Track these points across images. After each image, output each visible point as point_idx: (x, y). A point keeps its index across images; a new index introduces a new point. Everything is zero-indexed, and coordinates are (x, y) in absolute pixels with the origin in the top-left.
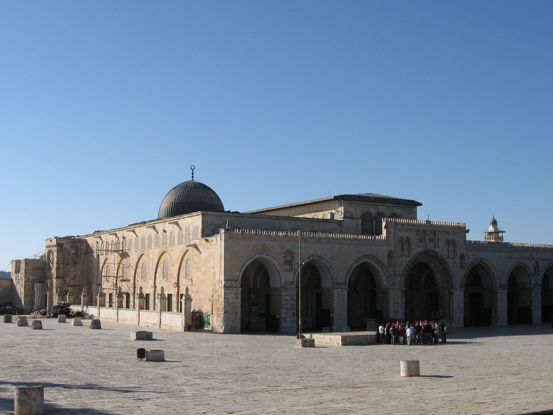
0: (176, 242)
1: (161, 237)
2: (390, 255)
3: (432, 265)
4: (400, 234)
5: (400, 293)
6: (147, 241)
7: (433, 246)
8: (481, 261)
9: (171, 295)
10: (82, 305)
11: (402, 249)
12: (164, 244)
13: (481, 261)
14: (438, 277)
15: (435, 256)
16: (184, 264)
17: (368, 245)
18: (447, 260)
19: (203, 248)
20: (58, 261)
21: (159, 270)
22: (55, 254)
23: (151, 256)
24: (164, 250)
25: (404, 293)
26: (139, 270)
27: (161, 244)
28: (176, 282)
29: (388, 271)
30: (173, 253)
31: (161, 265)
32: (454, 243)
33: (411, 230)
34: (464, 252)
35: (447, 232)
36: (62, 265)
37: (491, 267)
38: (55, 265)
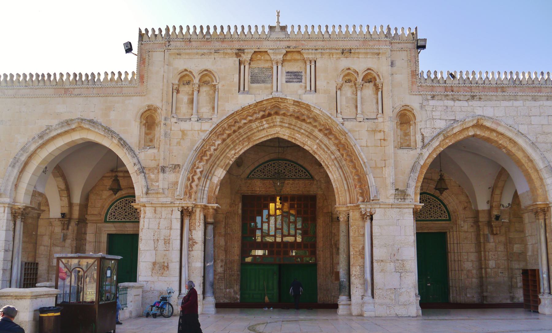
2: (149, 120)
3: (310, 146)
4: (181, 64)
5: (178, 215)
7: (301, 91)
8: (478, 125)
11: (191, 101)
13: (478, 125)
14: (334, 175)
15: (303, 115)
17: (79, 95)
18: (348, 125)
25: (199, 216)
29: (135, 155)
32: (370, 78)
33: (217, 51)
34: (414, 102)
35: (346, 52)
37: (520, 141)
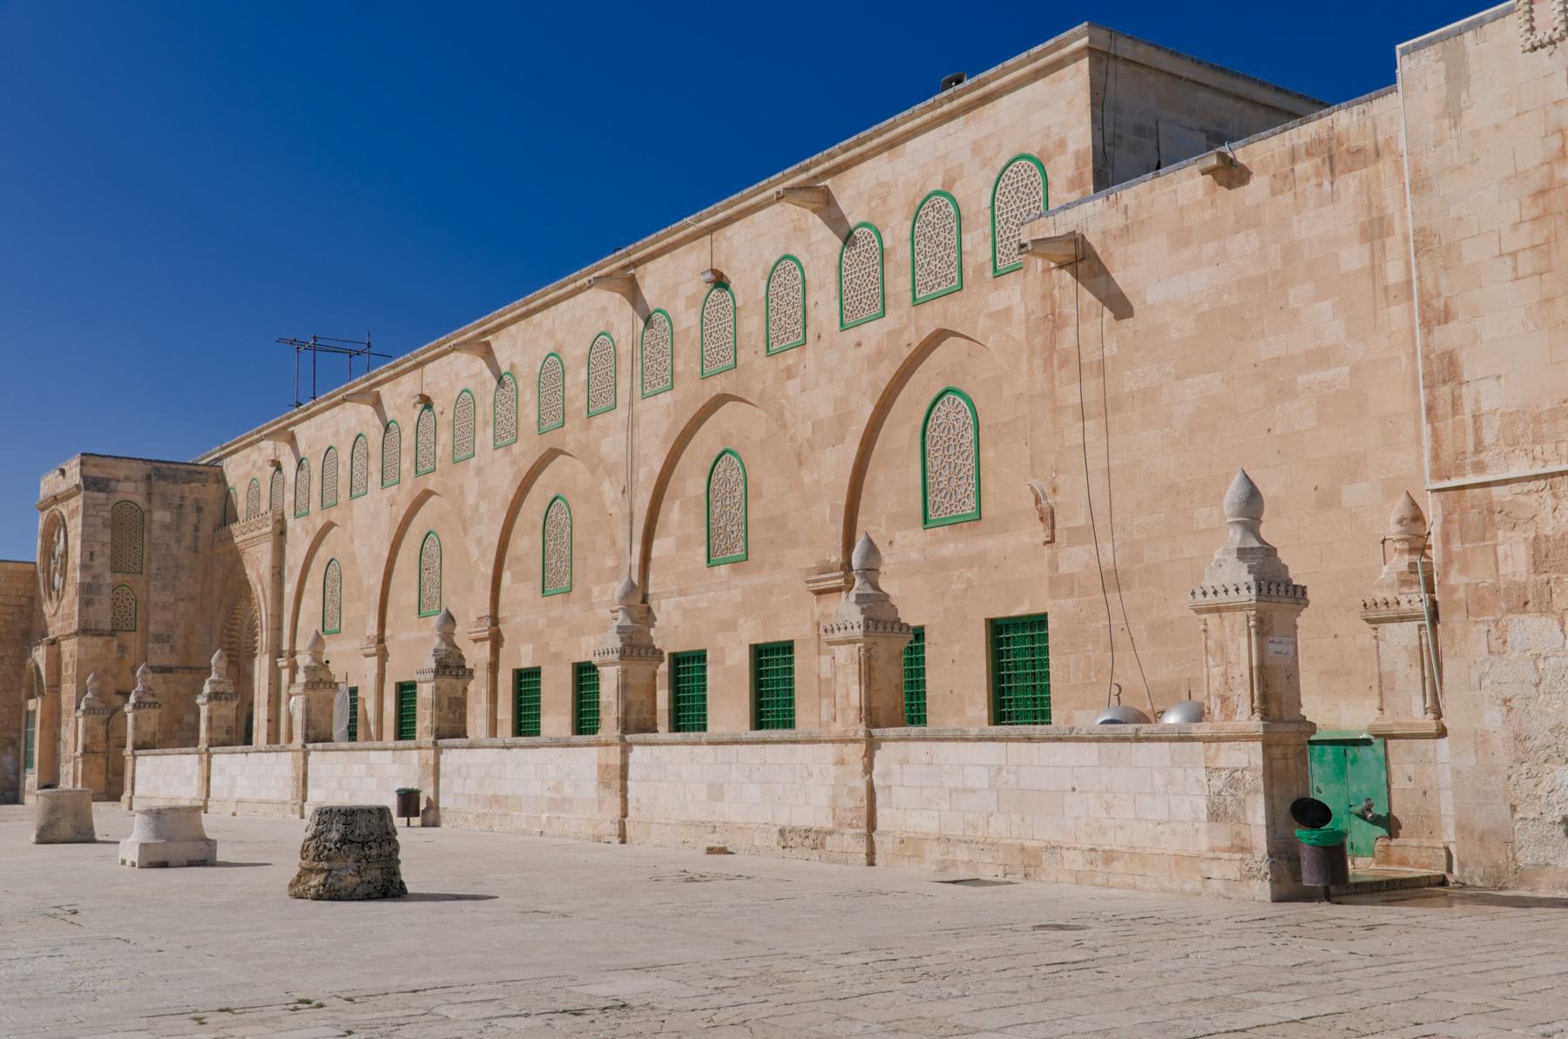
0: (824, 307)
1: (687, 320)
6: (577, 377)
9: (787, 648)
10: (203, 745)
12: (721, 354)
16: (901, 431)
19: (1181, 238)
20: (89, 556)
21: (672, 513)
22: (75, 527)
23: (612, 446)
24: (718, 386)
26: (525, 543)
27: (686, 362)
28: (836, 557)
30: (793, 386)
31: (690, 482)
36: (108, 578)
38: (75, 576)
